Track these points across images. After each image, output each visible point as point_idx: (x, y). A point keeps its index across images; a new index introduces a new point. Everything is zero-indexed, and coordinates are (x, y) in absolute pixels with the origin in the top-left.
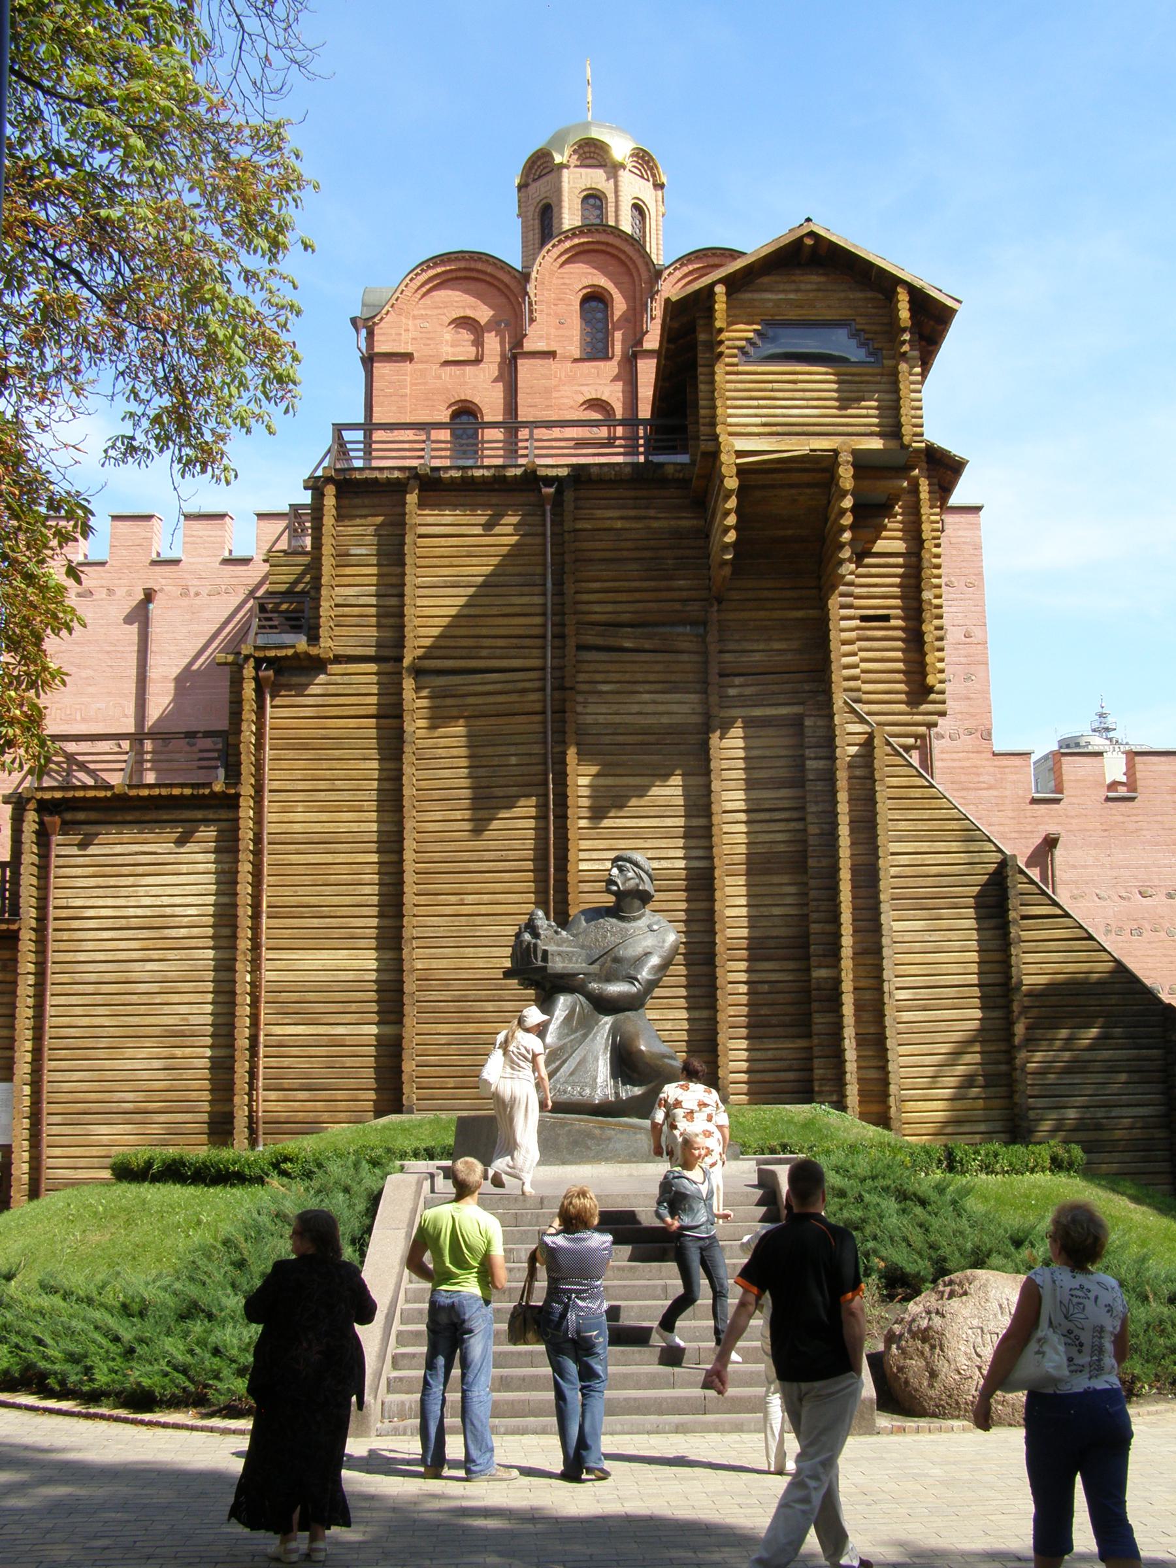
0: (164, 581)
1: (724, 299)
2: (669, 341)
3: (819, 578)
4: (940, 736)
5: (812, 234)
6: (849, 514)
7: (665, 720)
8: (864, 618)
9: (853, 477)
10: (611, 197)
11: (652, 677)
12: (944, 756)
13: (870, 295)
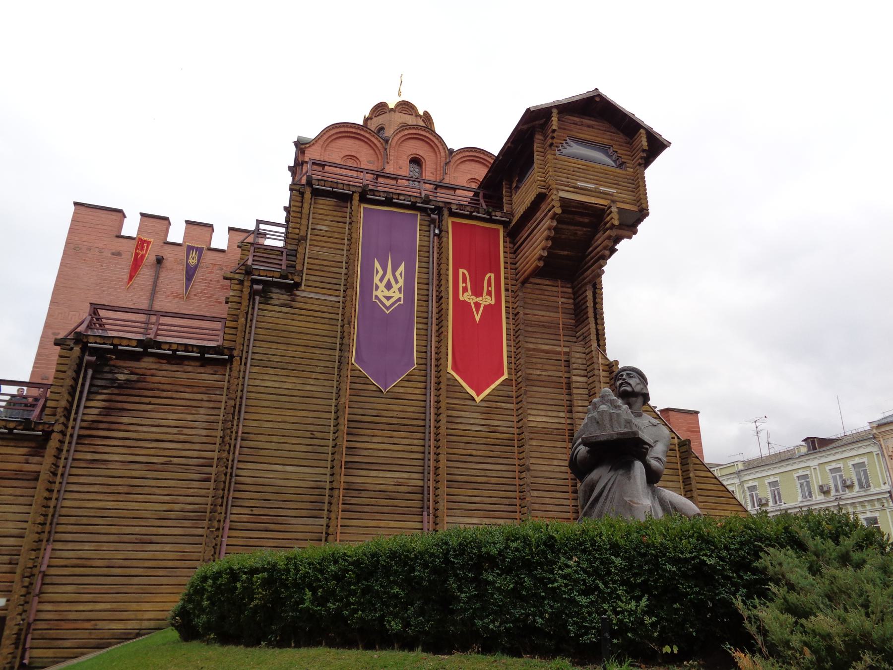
2: (512, 143)
5: (600, 96)
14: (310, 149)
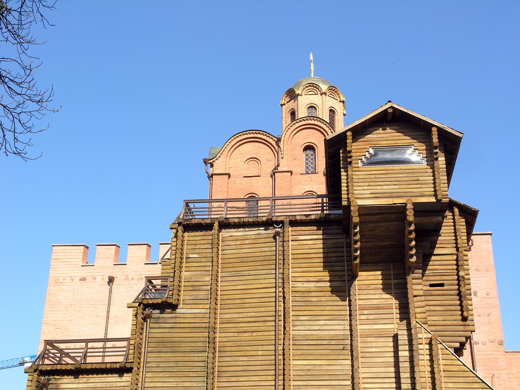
0: (118, 274)
1: (351, 138)
3: (404, 264)
4: (477, 343)
6: (413, 232)
7: (332, 333)
8: (431, 285)
9: (414, 215)
10: (320, 106)
11: (326, 313)
12: (479, 353)
13: (420, 133)
14: (217, 161)
